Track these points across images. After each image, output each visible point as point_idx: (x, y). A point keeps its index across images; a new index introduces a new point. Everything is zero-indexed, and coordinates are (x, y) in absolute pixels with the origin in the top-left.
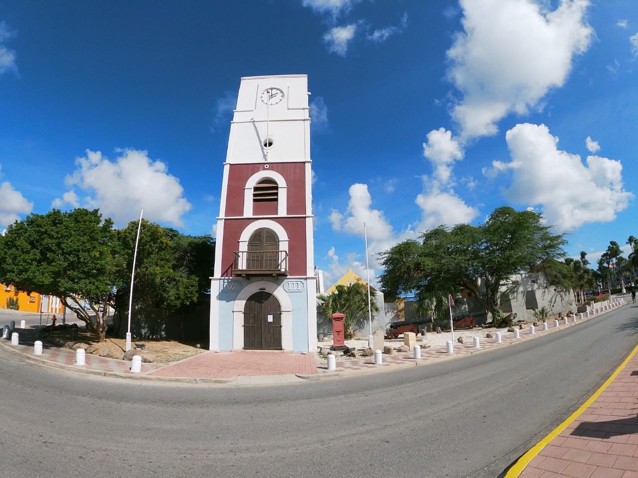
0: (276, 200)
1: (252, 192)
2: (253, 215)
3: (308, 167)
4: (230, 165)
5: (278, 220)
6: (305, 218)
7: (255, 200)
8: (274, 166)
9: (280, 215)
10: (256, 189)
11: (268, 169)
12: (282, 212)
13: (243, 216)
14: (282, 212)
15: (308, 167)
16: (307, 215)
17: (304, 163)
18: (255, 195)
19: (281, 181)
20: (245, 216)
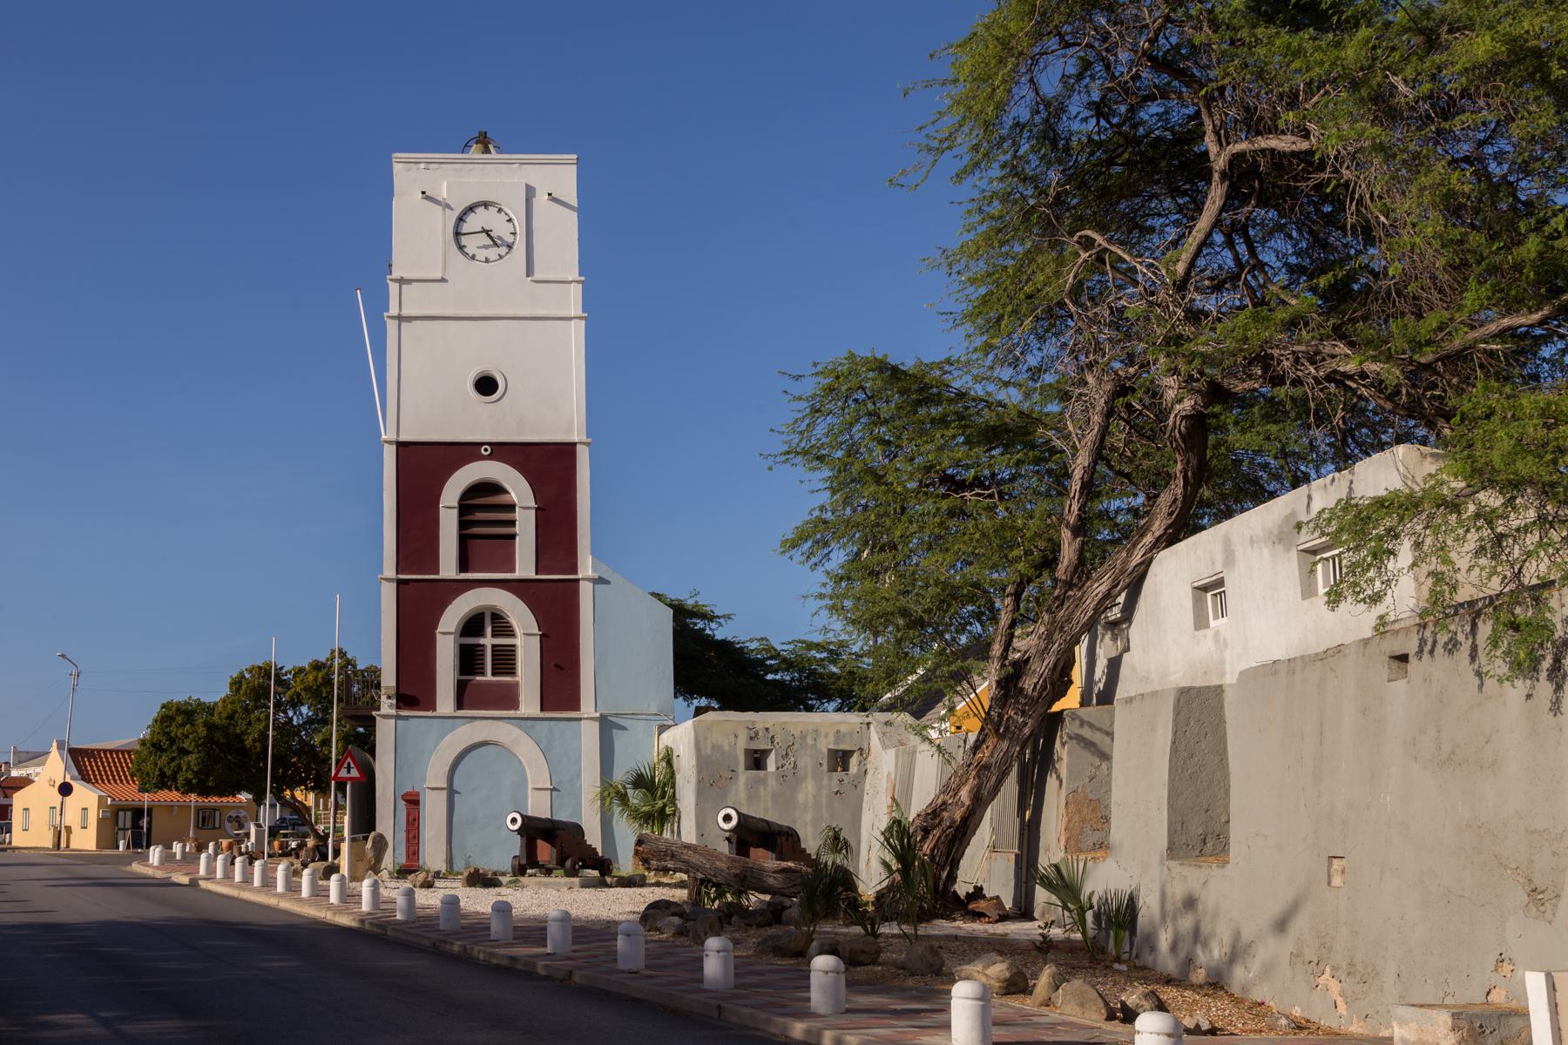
0: (513, 537)
1: (455, 513)
2: (460, 572)
6: (577, 581)
8: (503, 451)
11: (490, 457)
12: (525, 566)
13: (438, 574)
17: (574, 445)
19: (518, 490)
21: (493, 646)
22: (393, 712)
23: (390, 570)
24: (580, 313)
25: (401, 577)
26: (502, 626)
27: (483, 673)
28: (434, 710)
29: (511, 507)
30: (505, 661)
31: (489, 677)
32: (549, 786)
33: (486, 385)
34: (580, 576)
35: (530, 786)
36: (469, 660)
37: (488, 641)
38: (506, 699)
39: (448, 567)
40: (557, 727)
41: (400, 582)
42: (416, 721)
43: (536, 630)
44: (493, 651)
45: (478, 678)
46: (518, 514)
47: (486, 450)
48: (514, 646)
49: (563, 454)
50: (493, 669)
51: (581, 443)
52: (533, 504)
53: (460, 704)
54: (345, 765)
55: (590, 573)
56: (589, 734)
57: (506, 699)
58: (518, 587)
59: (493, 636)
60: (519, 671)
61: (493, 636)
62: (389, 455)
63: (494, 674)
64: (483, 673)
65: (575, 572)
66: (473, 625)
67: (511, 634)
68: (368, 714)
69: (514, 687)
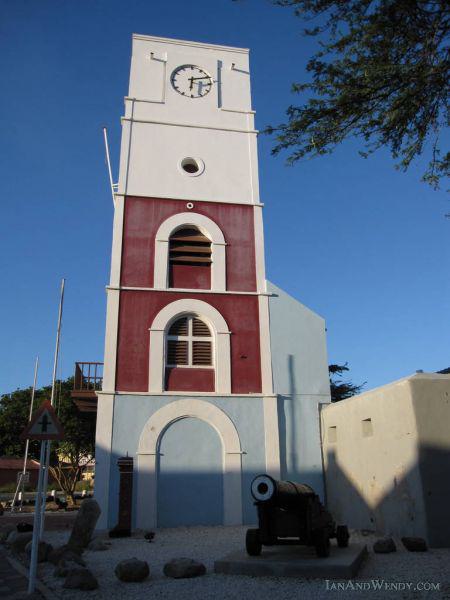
0: (209, 264)
1: (167, 244)
3: (258, 214)
8: (199, 207)
10: (173, 243)
12: (218, 284)
13: (152, 286)
14: (218, 284)
15: (258, 214)
16: (258, 293)
17: (251, 207)
23: (115, 280)
24: (253, 129)
25: (124, 288)
26: (201, 329)
27: (186, 363)
29: (208, 244)
30: (203, 353)
31: (190, 365)
32: (239, 451)
33: (190, 167)
34: (258, 293)
35: (224, 452)
36: (174, 352)
38: (205, 382)
40: (245, 401)
41: (121, 291)
42: (131, 398)
44: (194, 346)
45: (178, 366)
48: (209, 342)
50: (194, 360)
53: (167, 387)
54: (40, 420)
55: (265, 291)
56: (270, 407)
57: (205, 382)
58: (213, 300)
59: (194, 335)
60: (214, 362)
61: (194, 335)
62: (119, 205)
63: (194, 364)
64: (186, 363)
65: (255, 291)
66: (177, 326)
67: (208, 334)
68: (89, 395)
69: (211, 373)
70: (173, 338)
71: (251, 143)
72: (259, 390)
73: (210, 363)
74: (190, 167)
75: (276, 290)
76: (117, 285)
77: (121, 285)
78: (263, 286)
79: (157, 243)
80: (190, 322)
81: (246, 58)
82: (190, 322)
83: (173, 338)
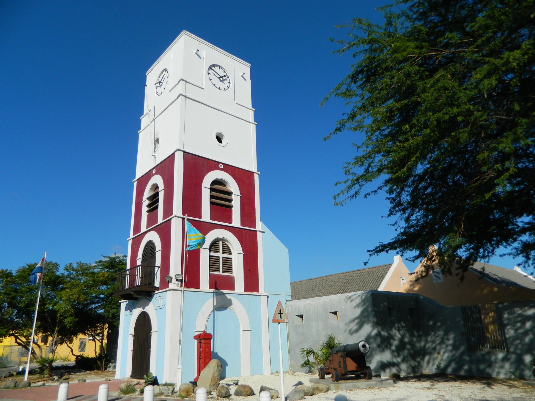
0: (231, 207)
1: (209, 190)
3: (256, 178)
4: (184, 152)
5: (233, 230)
6: (257, 231)
7: (211, 203)
8: (229, 169)
9: (233, 225)
10: (212, 190)
12: (236, 222)
14: (236, 222)
16: (257, 229)
17: (254, 173)
18: (212, 197)
19: (233, 186)
20: (203, 219)
21: (223, 258)
22: (179, 288)
26: (227, 250)
27: (218, 271)
28: (198, 288)
29: (230, 194)
30: (228, 265)
31: (221, 273)
33: (219, 139)
35: (241, 329)
36: (213, 263)
37: (221, 255)
39: (206, 216)
40: (251, 297)
42: (191, 294)
43: (241, 252)
44: (223, 260)
46: (233, 196)
47: (221, 166)
48: (231, 258)
49: (250, 175)
51: (256, 173)
52: (239, 194)
59: (223, 253)
61: (223, 253)
63: (223, 271)
65: (256, 228)
66: (214, 246)
67: (230, 253)
70: (212, 254)
71: (252, 129)
72: (257, 291)
73: (231, 272)
74: (219, 139)
75: (266, 229)
76: (180, 214)
77: (183, 214)
78: (259, 226)
79: (203, 188)
80: (221, 243)
81: (248, 70)
82: (221, 243)
83: (212, 254)
